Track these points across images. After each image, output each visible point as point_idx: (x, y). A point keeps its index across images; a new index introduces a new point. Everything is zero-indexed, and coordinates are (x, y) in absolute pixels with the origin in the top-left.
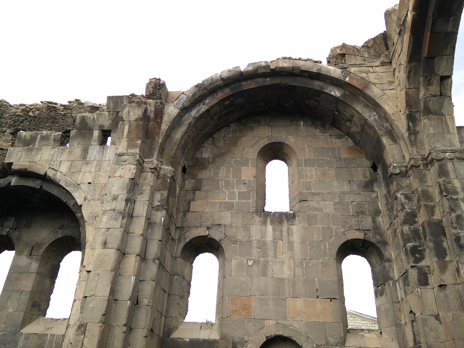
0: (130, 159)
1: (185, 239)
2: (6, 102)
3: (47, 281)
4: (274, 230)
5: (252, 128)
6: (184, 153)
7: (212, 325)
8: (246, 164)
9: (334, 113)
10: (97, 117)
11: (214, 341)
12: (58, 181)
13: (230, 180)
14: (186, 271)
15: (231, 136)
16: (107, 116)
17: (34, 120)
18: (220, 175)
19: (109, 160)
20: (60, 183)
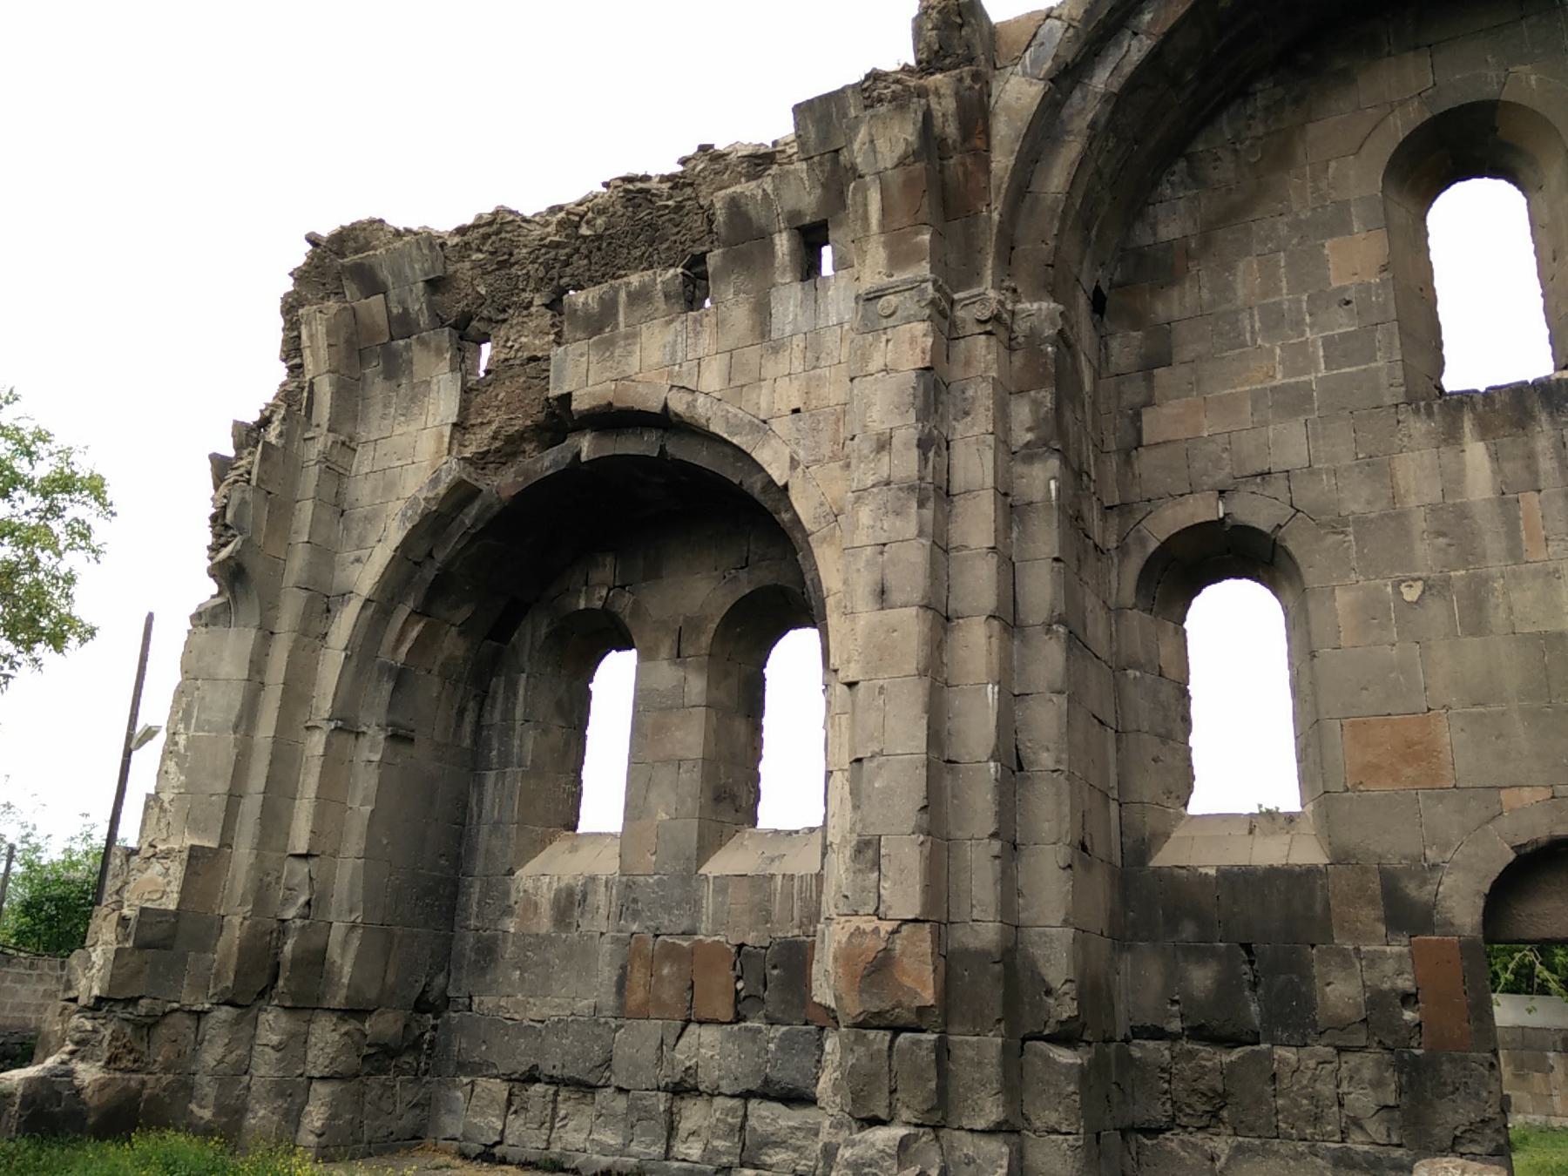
0: (907, 303)
1: (1142, 542)
2: (511, 212)
3: (740, 726)
4: (1495, 457)
5: (1346, 78)
6: (1086, 241)
7: (1291, 818)
8: (1340, 226)
10: (776, 189)
11: (1311, 872)
12: (703, 421)
13: (1280, 304)
14: (1166, 651)
15: (1260, 129)
16: (804, 175)
17: (599, 249)
18: (1241, 292)
19: (841, 324)
20: (712, 428)
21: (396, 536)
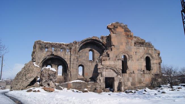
21: (42, 60)
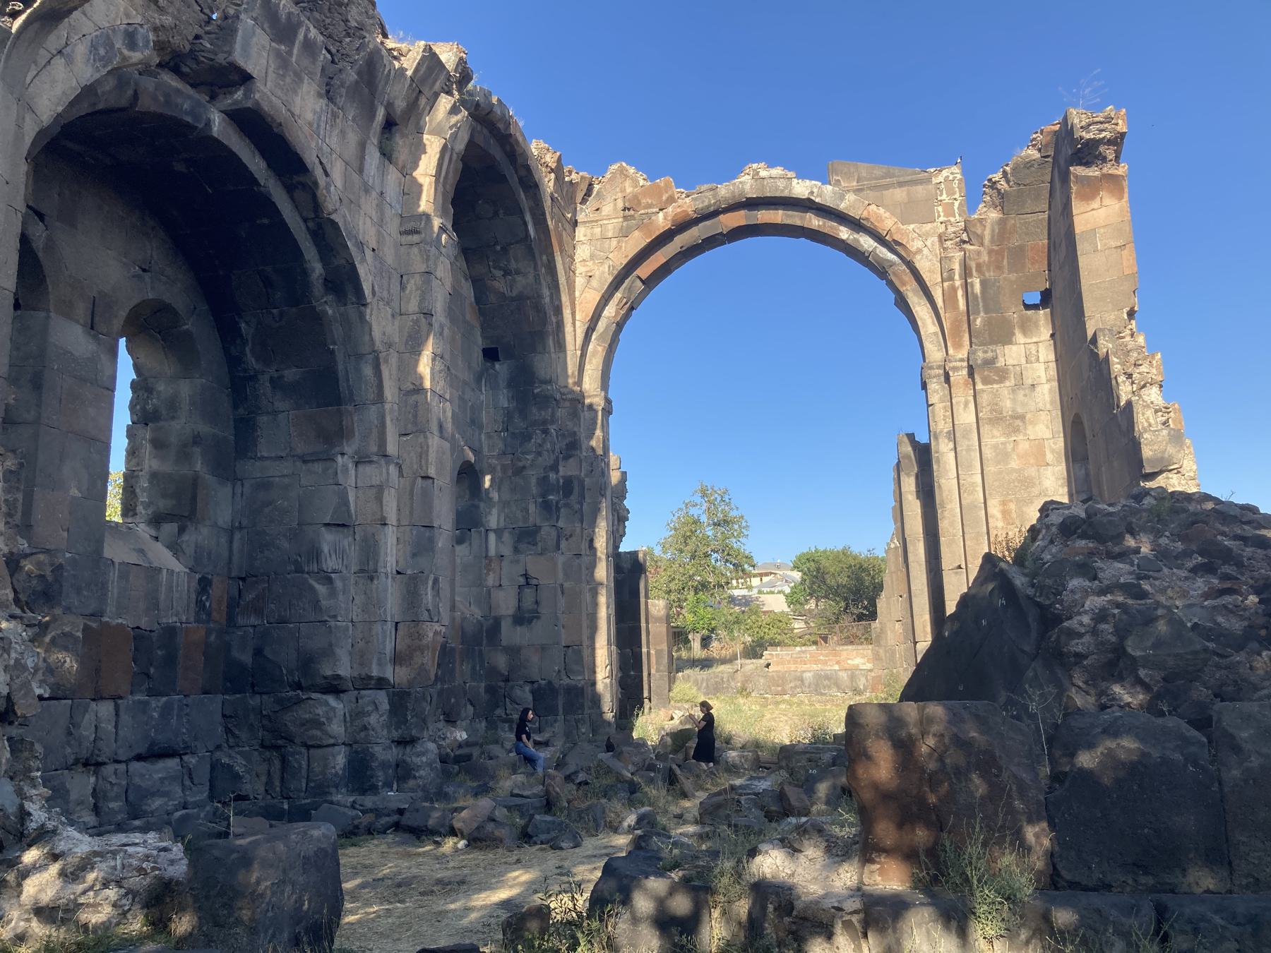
9: (496, 243)
